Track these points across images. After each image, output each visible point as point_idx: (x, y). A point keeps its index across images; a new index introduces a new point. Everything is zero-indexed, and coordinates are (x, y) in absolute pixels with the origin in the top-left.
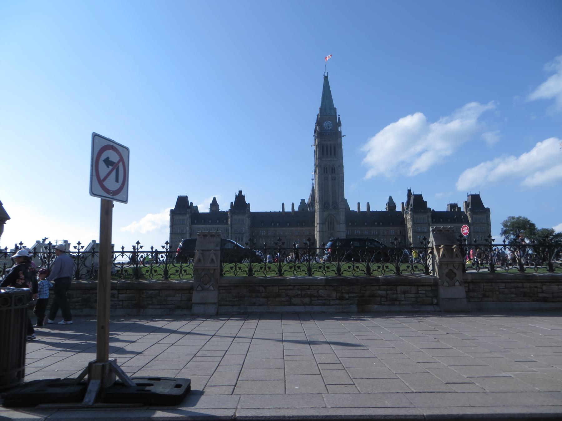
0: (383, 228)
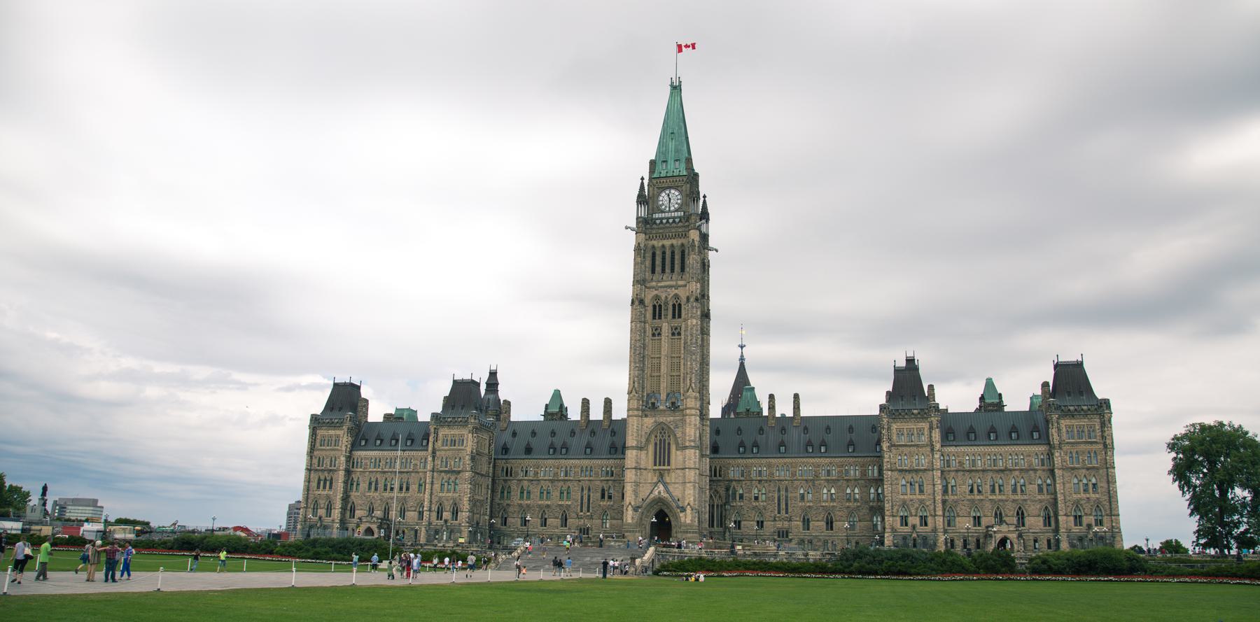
0: (828, 460)
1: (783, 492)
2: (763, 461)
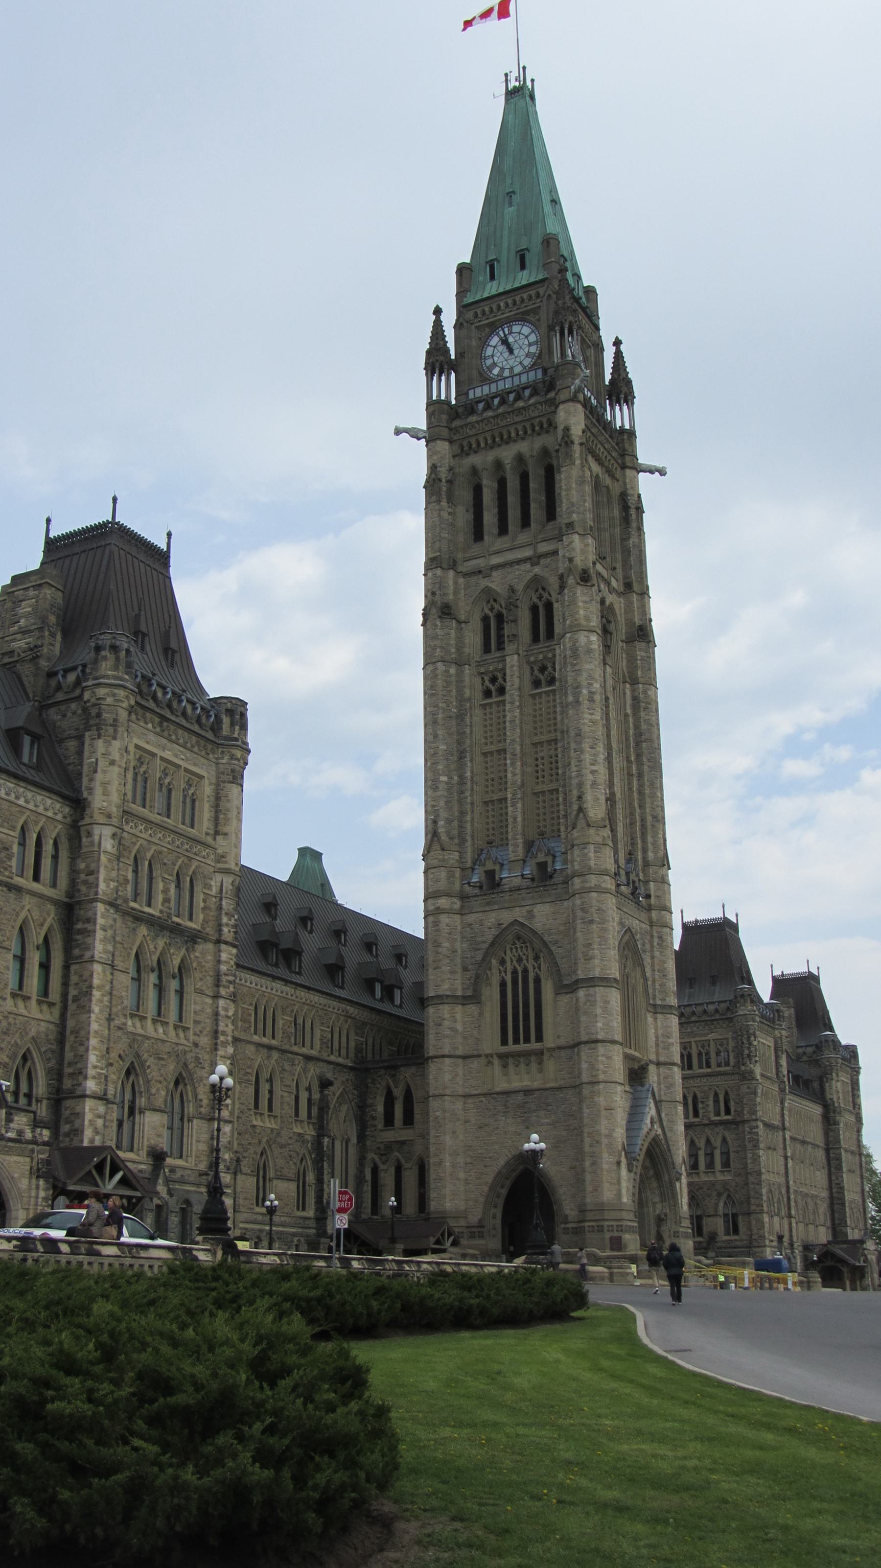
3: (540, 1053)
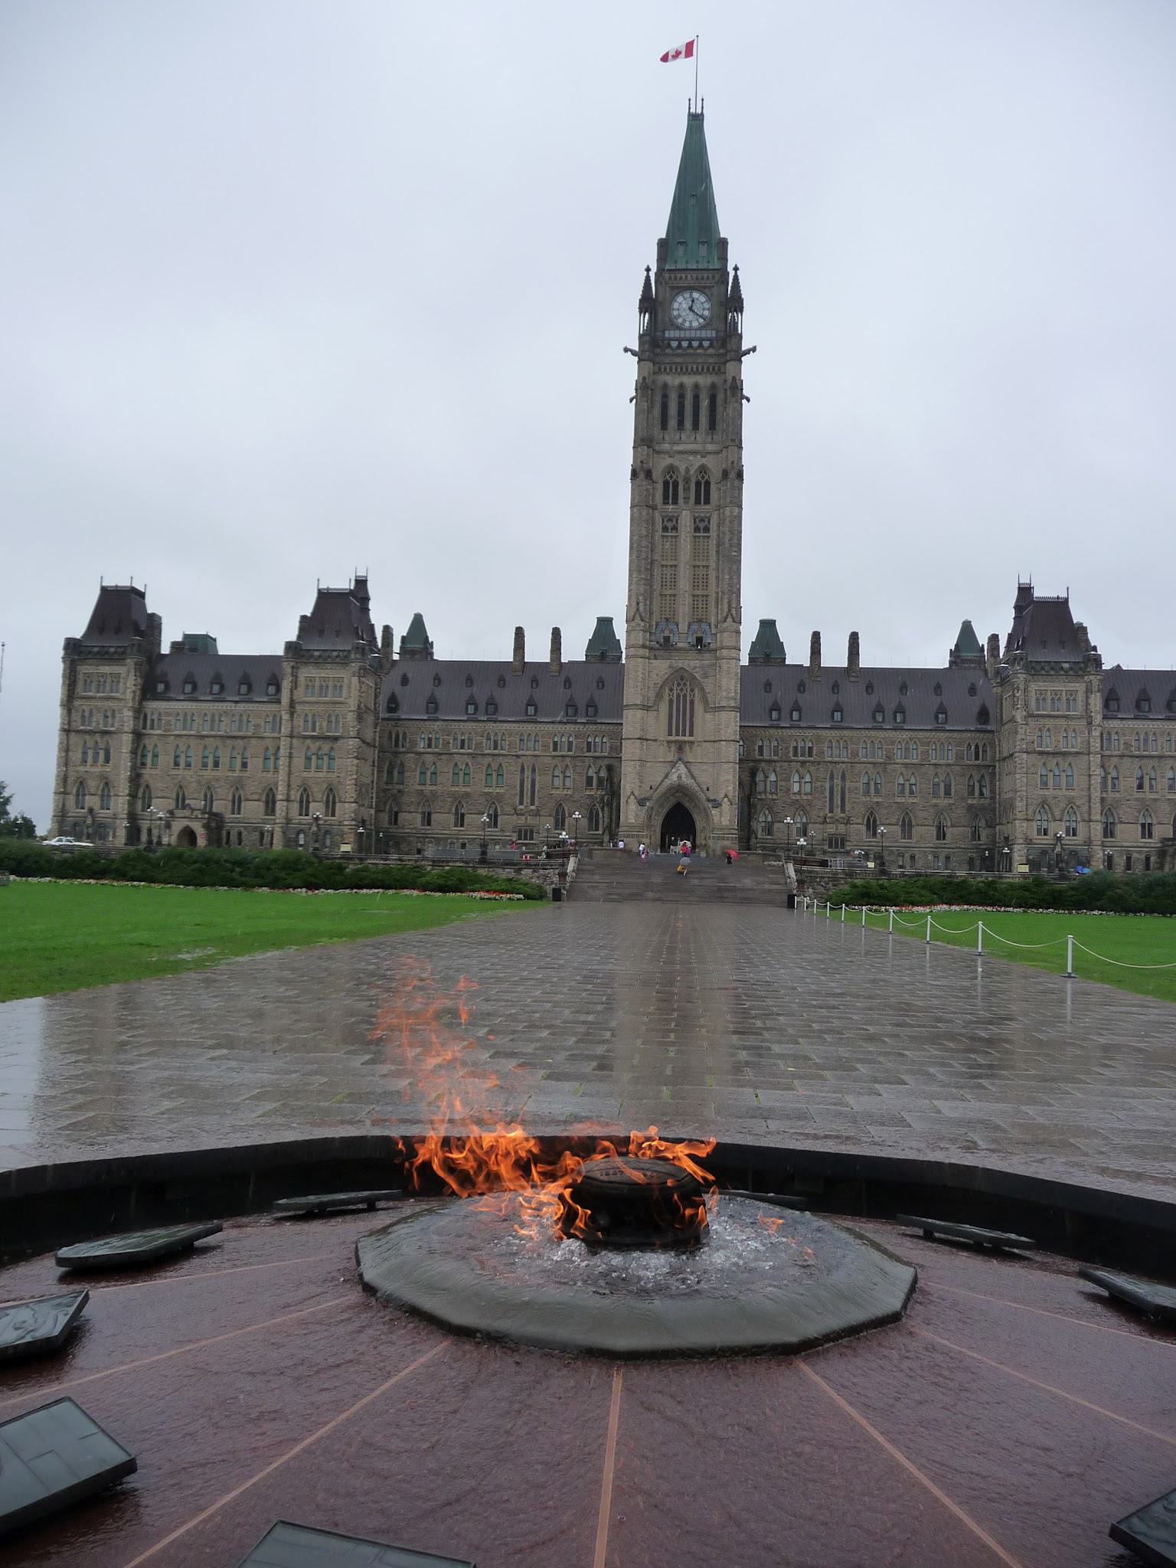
0: (906, 735)
1: (838, 781)
2: (810, 733)
3: (692, 743)
